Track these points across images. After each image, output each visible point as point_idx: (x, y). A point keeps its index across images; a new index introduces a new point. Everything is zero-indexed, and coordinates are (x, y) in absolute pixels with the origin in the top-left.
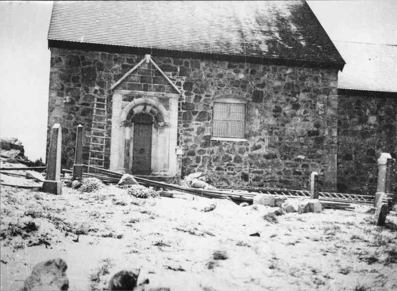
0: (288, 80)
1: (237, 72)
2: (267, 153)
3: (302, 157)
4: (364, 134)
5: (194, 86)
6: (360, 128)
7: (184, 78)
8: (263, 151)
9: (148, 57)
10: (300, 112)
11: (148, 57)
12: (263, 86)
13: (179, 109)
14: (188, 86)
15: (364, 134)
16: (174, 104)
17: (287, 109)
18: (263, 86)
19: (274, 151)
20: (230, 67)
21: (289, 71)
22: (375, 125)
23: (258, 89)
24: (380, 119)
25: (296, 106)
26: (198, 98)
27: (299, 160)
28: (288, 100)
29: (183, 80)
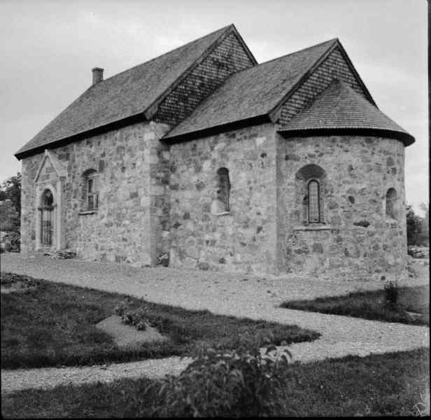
0: (119, 143)
1: (91, 147)
2: (107, 222)
3: (127, 222)
4: (199, 187)
5: (73, 169)
6: (194, 179)
7: (68, 162)
8: (105, 220)
9: (47, 152)
10: (126, 175)
11: (46, 150)
12: (103, 155)
13: (64, 190)
14: (69, 168)
15: (199, 187)
16: (59, 185)
17: (118, 174)
18: (103, 155)
19: (112, 219)
20: (88, 143)
21: (118, 134)
22: (208, 172)
23: (102, 159)
24: (214, 161)
25: (123, 169)
26: (74, 177)
27: (124, 225)
28: (118, 164)
29: (66, 164)
